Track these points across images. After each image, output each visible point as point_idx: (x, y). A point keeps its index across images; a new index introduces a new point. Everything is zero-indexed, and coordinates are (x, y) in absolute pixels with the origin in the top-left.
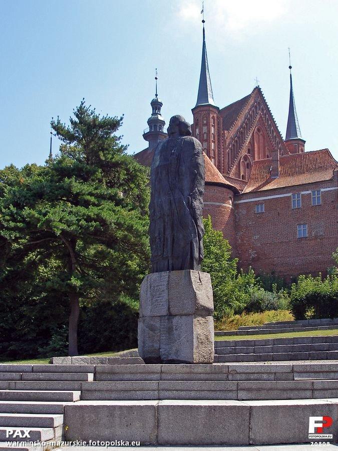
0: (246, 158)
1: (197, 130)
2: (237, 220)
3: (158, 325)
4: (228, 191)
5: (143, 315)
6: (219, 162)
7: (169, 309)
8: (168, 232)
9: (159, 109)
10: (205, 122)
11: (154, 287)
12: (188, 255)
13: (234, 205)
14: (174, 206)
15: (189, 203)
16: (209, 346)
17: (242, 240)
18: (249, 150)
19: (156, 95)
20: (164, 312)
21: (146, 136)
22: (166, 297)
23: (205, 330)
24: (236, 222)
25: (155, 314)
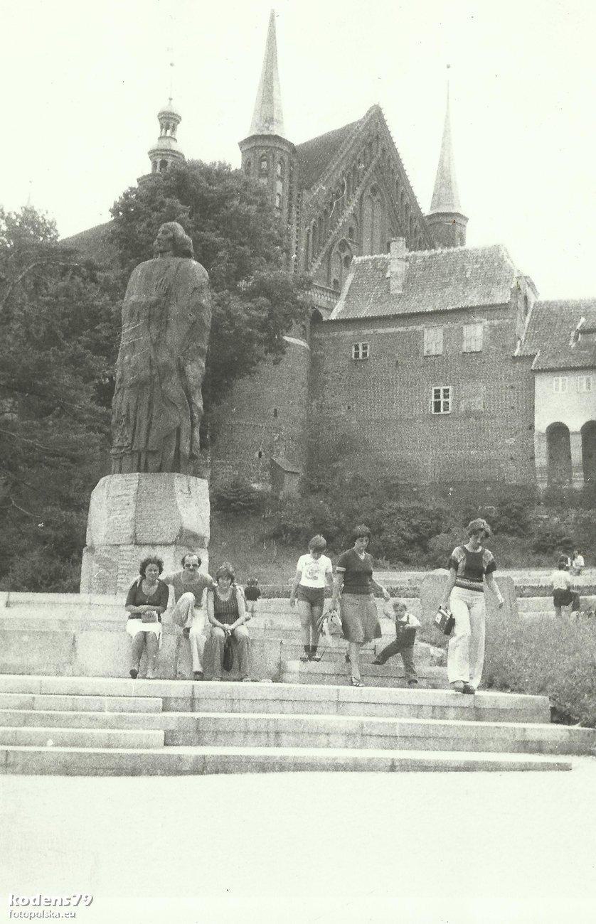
9: (174, 129)
18: (351, 230)
22: (131, 515)
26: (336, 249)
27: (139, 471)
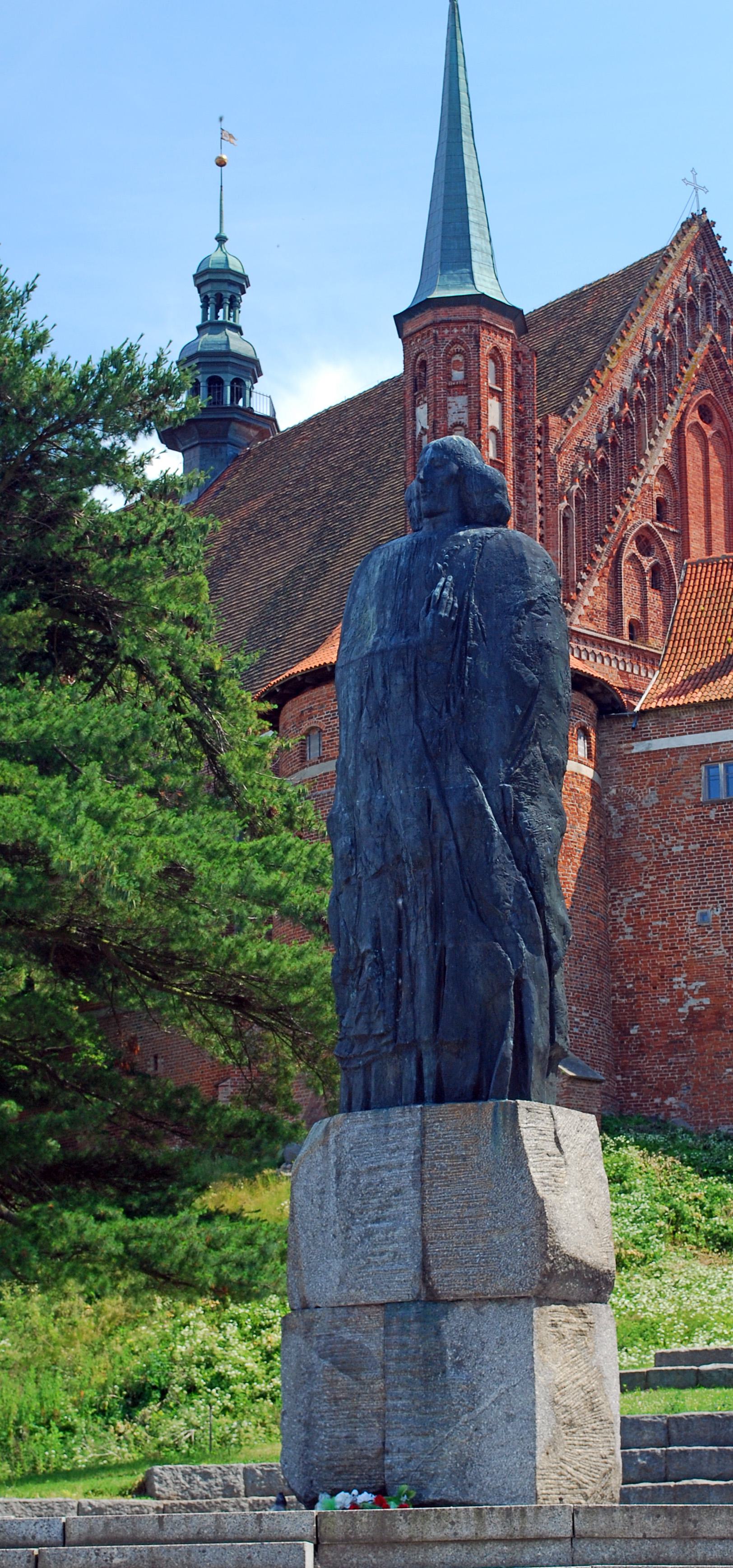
0: (646, 541)
1: (422, 412)
2: (615, 836)
3: (374, 1346)
7: (425, 1269)
8: (418, 934)
9: (234, 304)
10: (458, 375)
12: (503, 1037)
14: (442, 825)
16: (599, 1438)
17: (640, 928)
18: (661, 503)
19: (221, 240)
20: (403, 1285)
24: (609, 841)
25: (363, 1296)
26: (630, 549)
27: (419, 1098)
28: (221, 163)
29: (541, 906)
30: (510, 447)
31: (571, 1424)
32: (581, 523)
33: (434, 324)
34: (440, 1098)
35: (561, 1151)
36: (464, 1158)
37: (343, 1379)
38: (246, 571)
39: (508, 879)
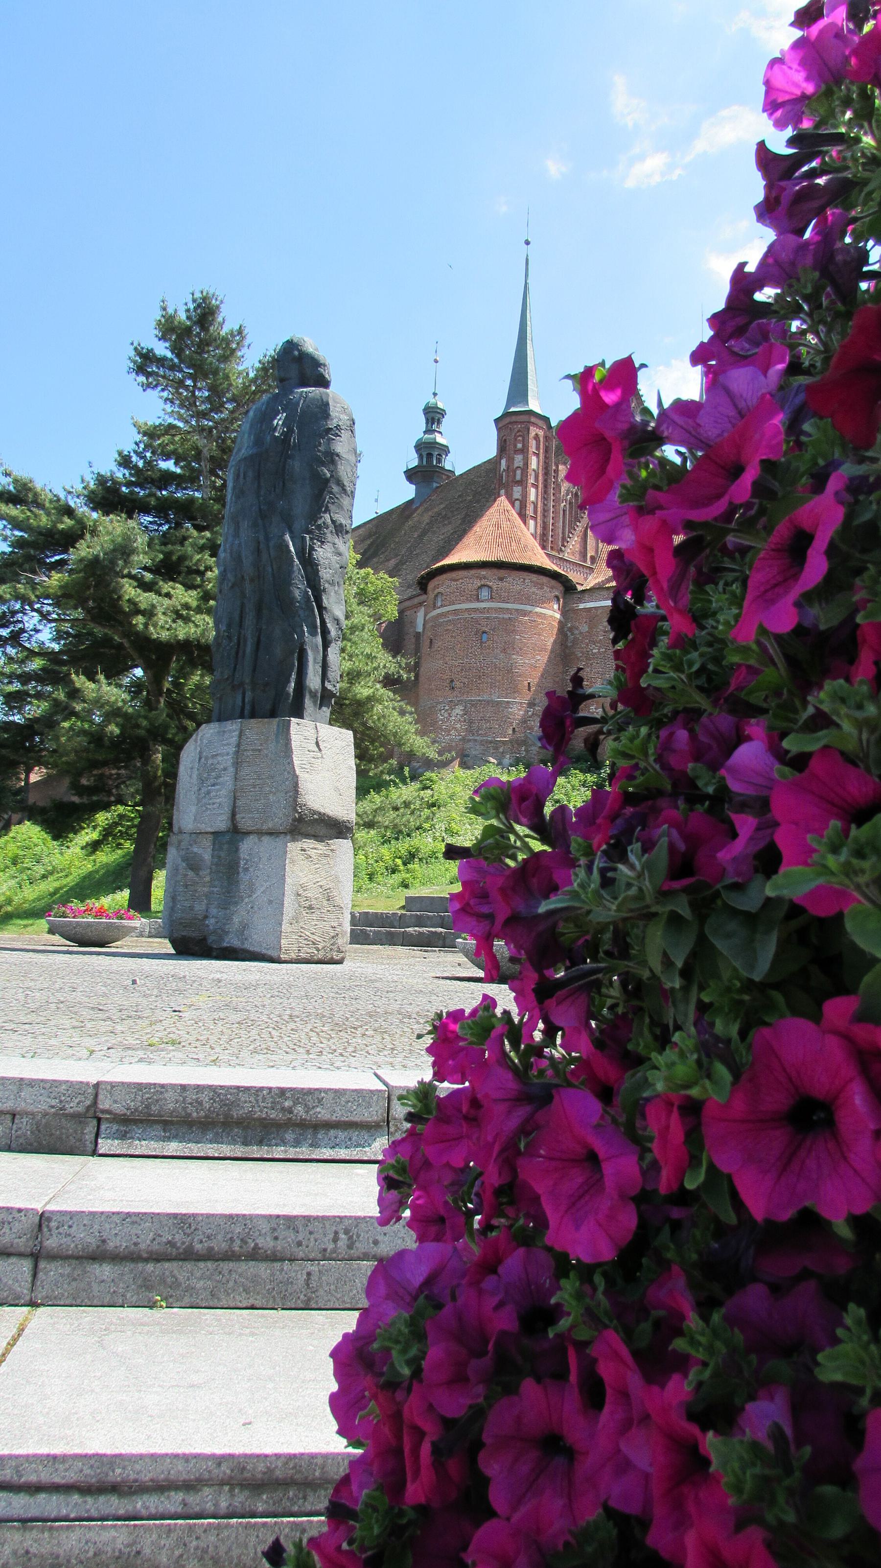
4: (553, 582)
5: (179, 828)
6: (545, 527)
8: (249, 621)
9: (439, 422)
11: (207, 758)
12: (289, 682)
13: (564, 612)
14: (265, 556)
15: (304, 549)
16: (332, 916)
19: (435, 394)
20: (221, 823)
21: (411, 475)
23: (323, 874)
24: (567, 647)
27: (242, 716)
28: (436, 361)
29: (321, 608)
30: (540, 478)
31: (310, 907)
32: (571, 513)
33: (510, 423)
34: (253, 715)
35: (320, 750)
36: (260, 750)
37: (191, 874)
38: (434, 533)
39: (299, 588)
